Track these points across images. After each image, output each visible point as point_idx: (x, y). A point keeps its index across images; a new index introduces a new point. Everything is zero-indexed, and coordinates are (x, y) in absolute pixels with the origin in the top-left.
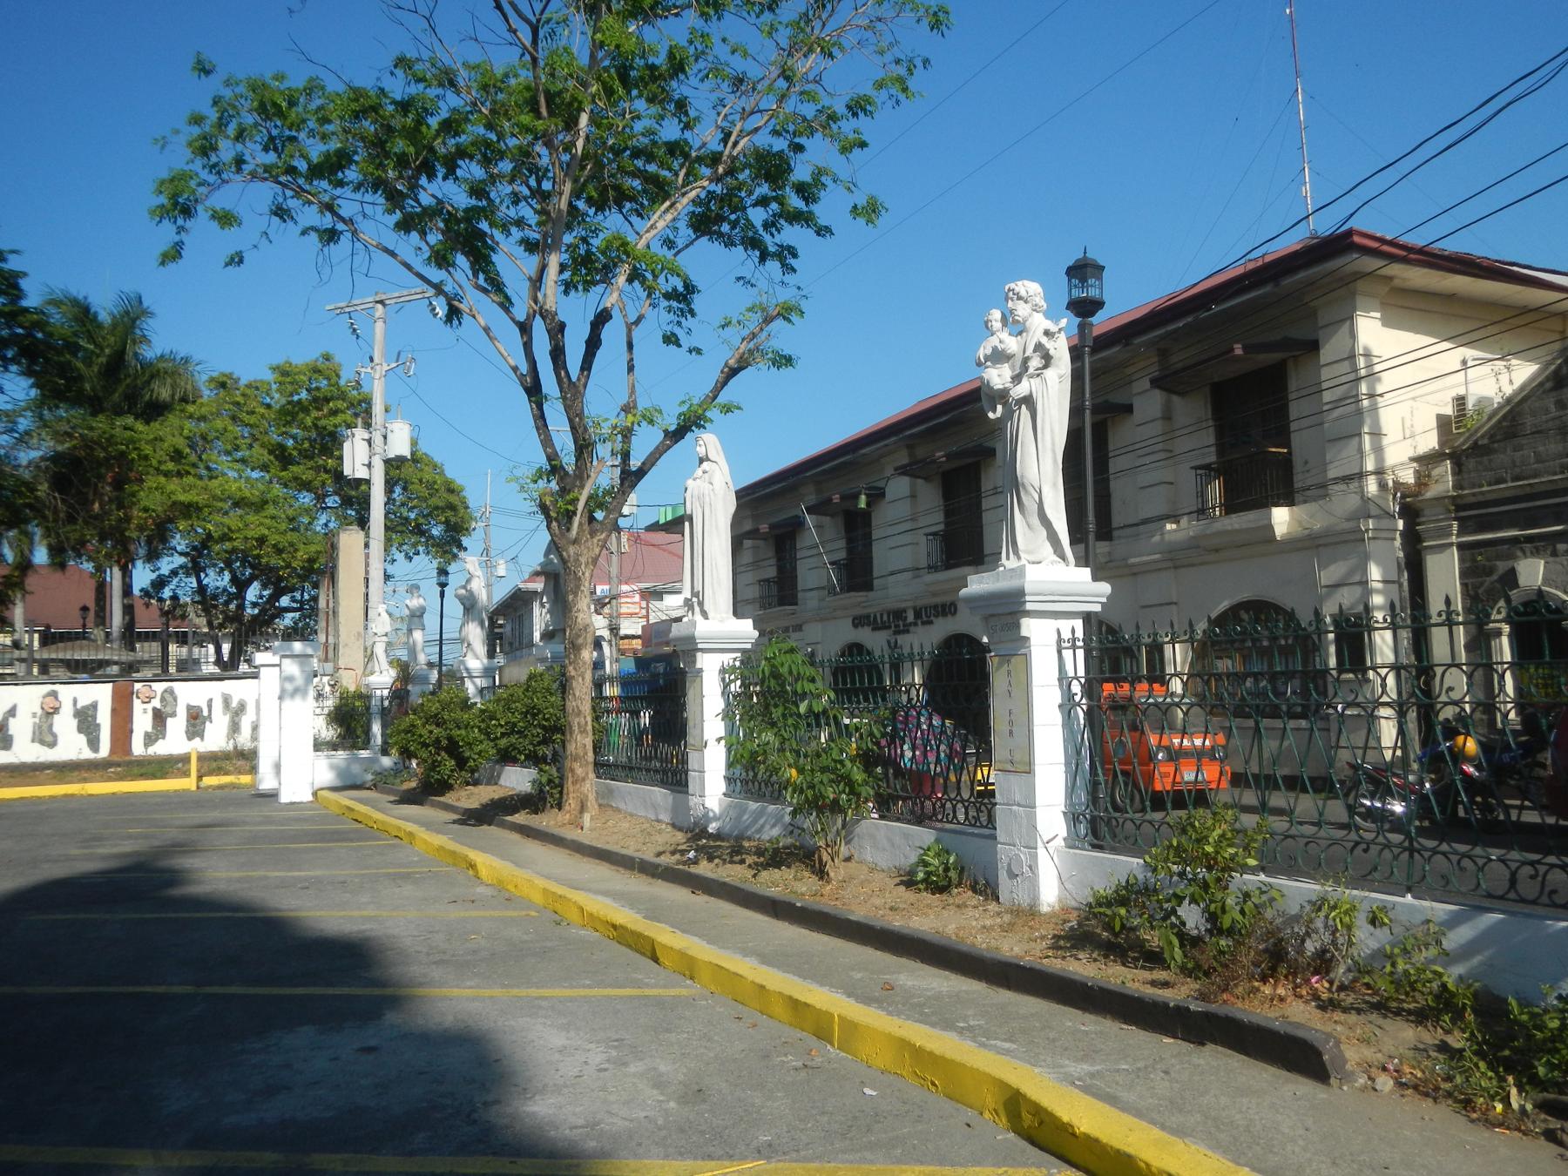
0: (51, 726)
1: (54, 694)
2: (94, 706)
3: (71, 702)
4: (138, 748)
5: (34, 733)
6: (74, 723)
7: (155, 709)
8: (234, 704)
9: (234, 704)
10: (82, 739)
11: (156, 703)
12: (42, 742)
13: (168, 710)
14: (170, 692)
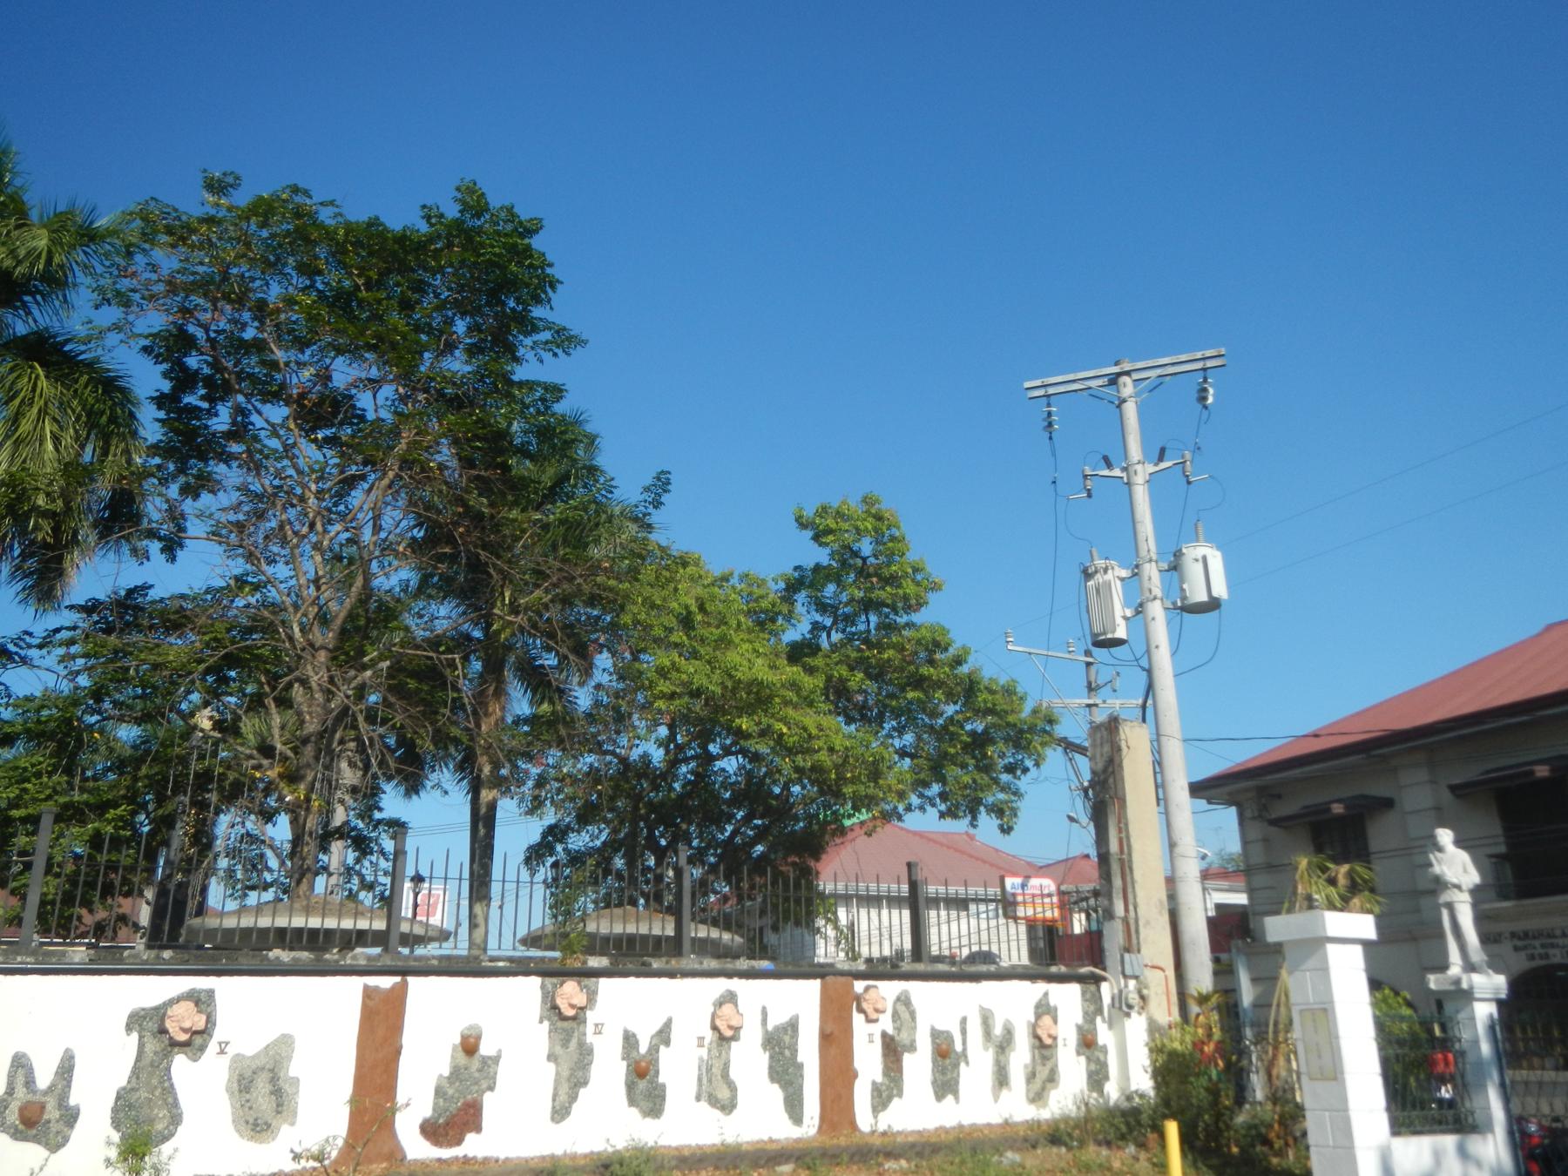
0: (726, 1066)
1: (730, 998)
2: (792, 1026)
3: (759, 1017)
4: (864, 1118)
5: (700, 1080)
6: (763, 1059)
7: (884, 1035)
8: (998, 1030)
9: (998, 1030)
10: (776, 1093)
11: (886, 1023)
12: (714, 1101)
13: (904, 1037)
14: (904, 1000)
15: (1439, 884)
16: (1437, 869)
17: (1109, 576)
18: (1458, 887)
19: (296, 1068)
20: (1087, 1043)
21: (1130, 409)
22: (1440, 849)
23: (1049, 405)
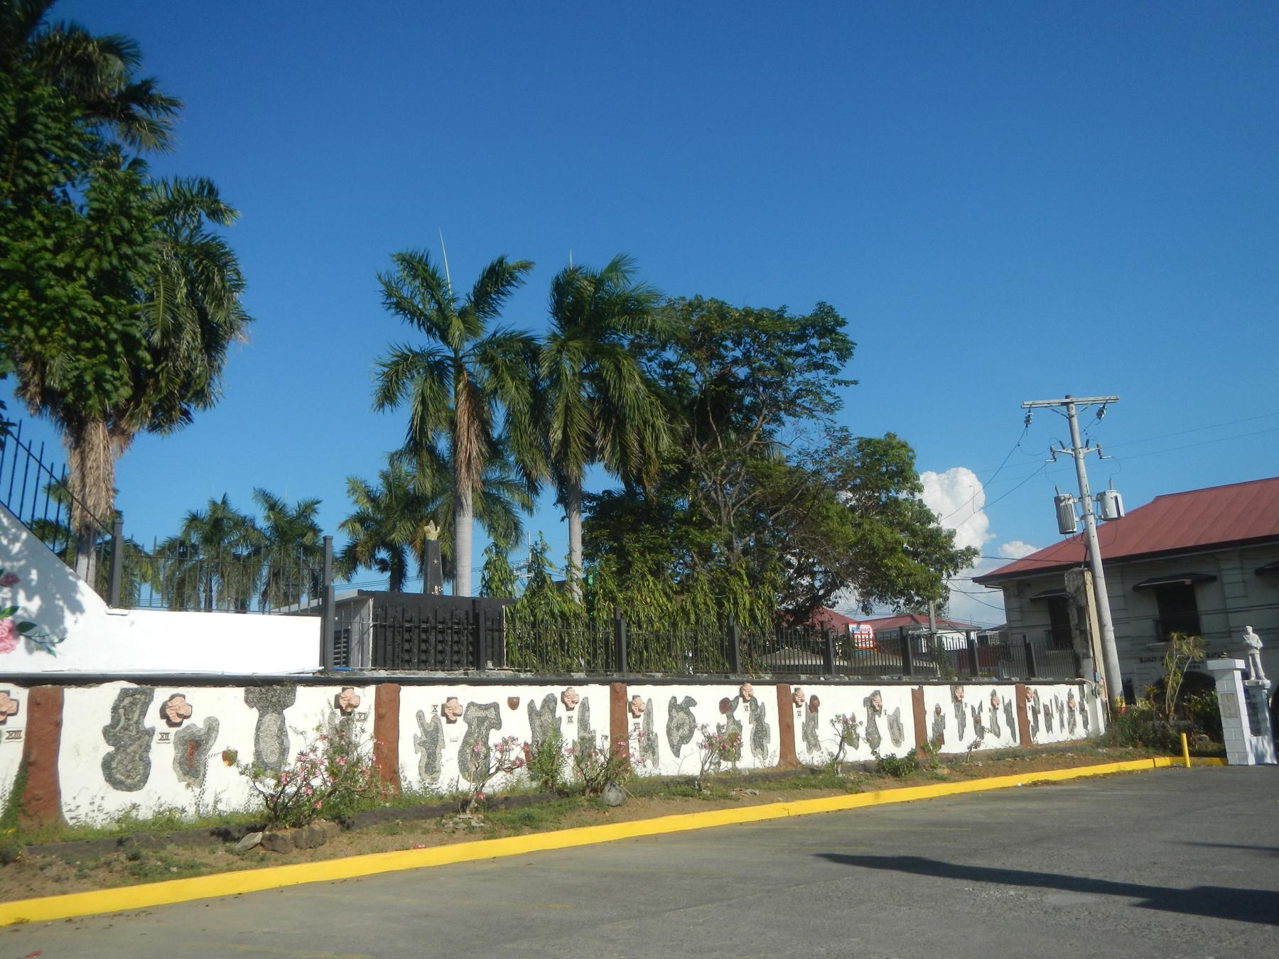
2: (1010, 703)
9: (1060, 705)
10: (1008, 728)
15: (1249, 647)
16: (1249, 642)
17: (1071, 502)
18: (1256, 648)
19: (902, 720)
20: (1082, 710)
21: (1075, 420)
22: (1248, 634)
23: (1029, 412)
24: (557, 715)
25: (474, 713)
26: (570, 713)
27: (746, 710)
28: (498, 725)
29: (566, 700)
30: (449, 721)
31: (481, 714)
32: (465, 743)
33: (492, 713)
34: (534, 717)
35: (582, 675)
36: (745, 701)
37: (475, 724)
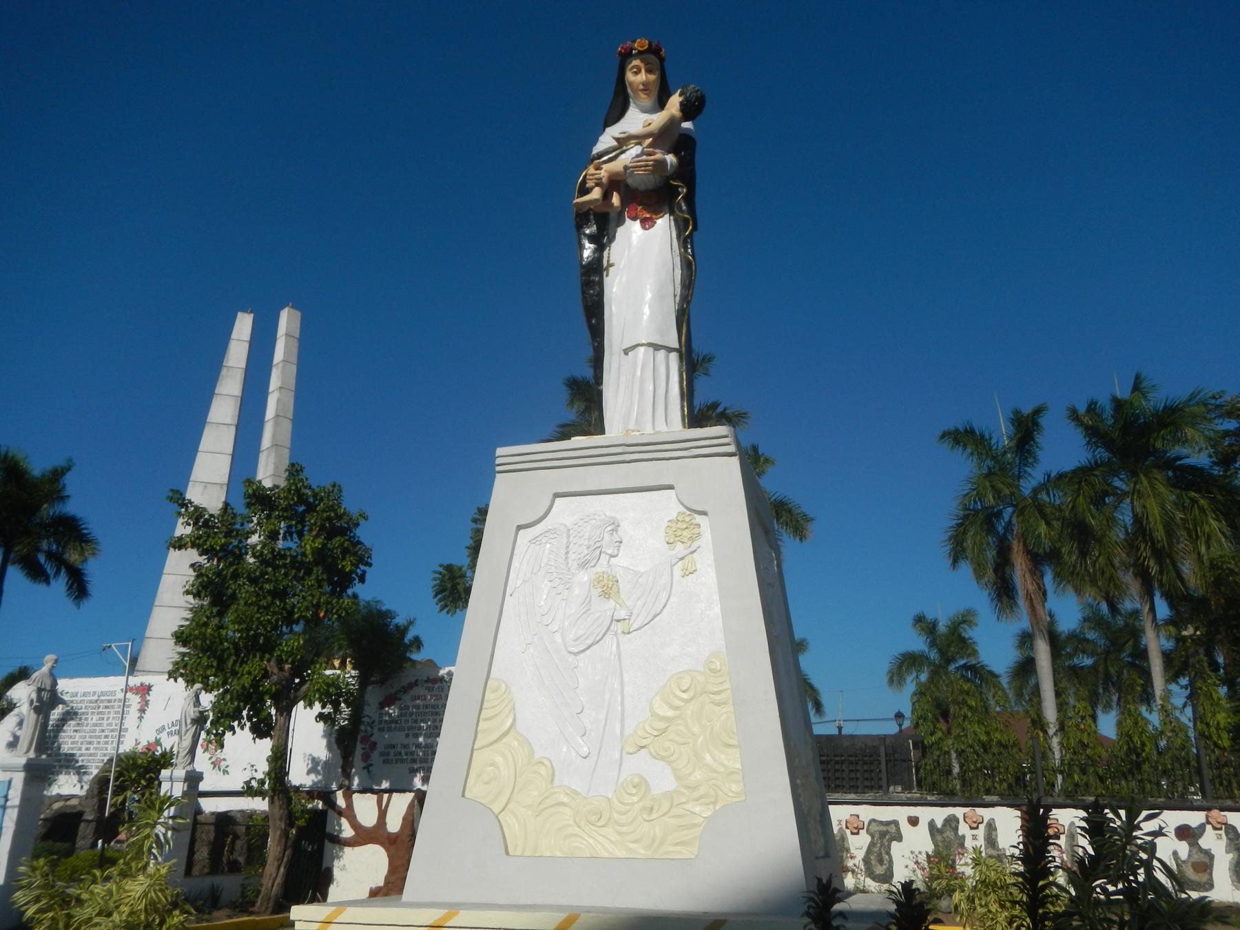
24: (960, 833)
25: (874, 827)
26: (974, 832)
27: (1219, 837)
28: (899, 838)
29: (967, 820)
30: (852, 833)
31: (883, 828)
32: (869, 852)
33: (892, 829)
34: (936, 833)
35: (995, 798)
36: (1215, 828)
37: (877, 836)
